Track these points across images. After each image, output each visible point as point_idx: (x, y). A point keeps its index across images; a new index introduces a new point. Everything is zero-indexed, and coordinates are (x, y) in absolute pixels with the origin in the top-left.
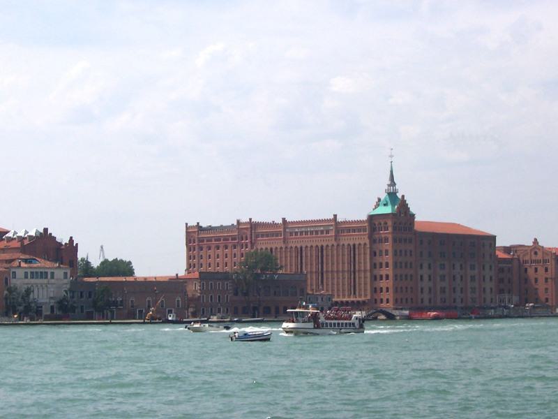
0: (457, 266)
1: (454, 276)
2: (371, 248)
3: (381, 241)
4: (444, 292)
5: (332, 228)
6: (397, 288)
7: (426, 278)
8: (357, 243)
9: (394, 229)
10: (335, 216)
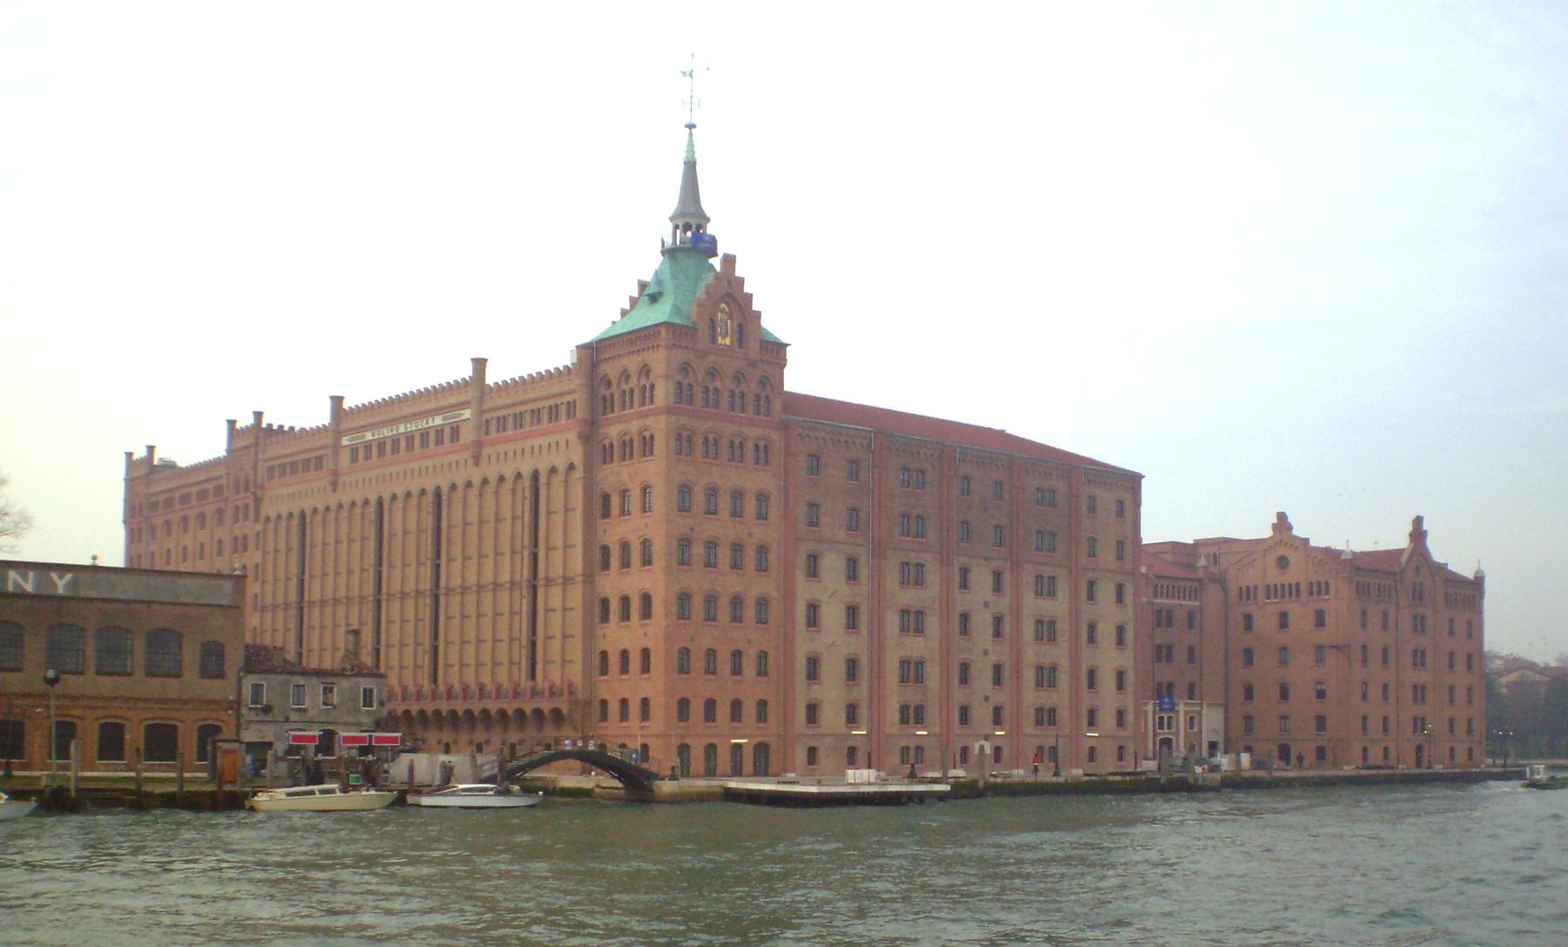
0: (981, 578)
1: (965, 617)
2: (589, 484)
4: (919, 679)
5: (467, 414)
6: (685, 652)
7: (832, 615)
8: (543, 467)
9: (683, 393)
10: (480, 364)
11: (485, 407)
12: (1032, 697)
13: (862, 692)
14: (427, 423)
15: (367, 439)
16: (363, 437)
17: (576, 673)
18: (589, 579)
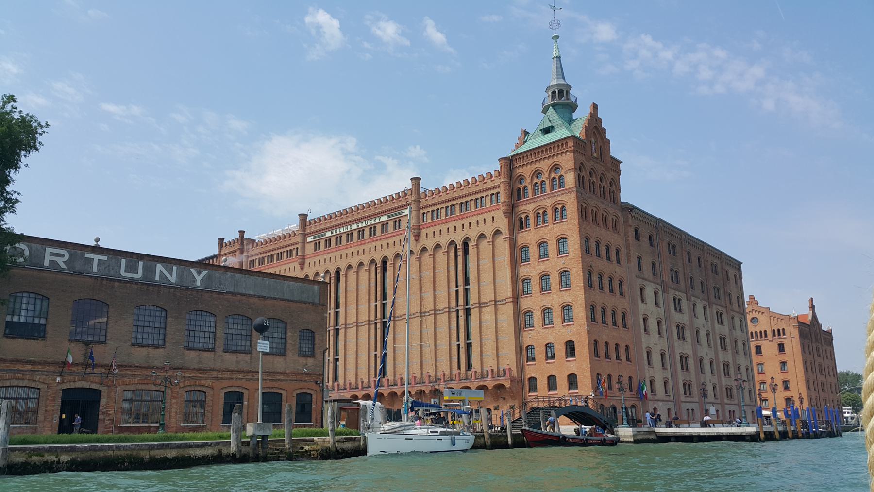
2: (512, 240)
3: (540, 216)
8: (473, 235)
11: (422, 205)
13: (668, 374)
14: (375, 221)
15: (327, 236)
16: (325, 235)
17: (509, 359)
18: (516, 300)
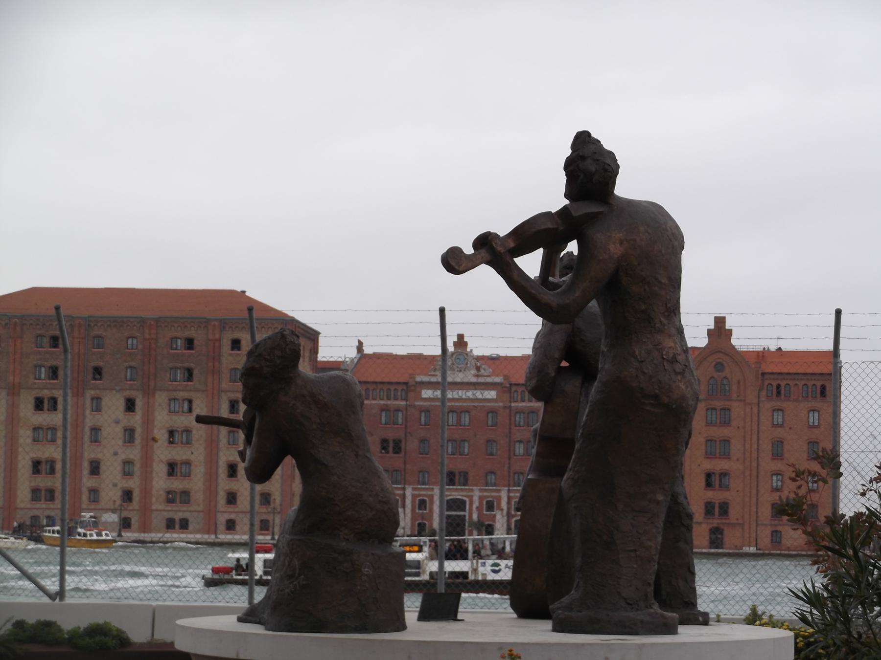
12: (161, 482)
